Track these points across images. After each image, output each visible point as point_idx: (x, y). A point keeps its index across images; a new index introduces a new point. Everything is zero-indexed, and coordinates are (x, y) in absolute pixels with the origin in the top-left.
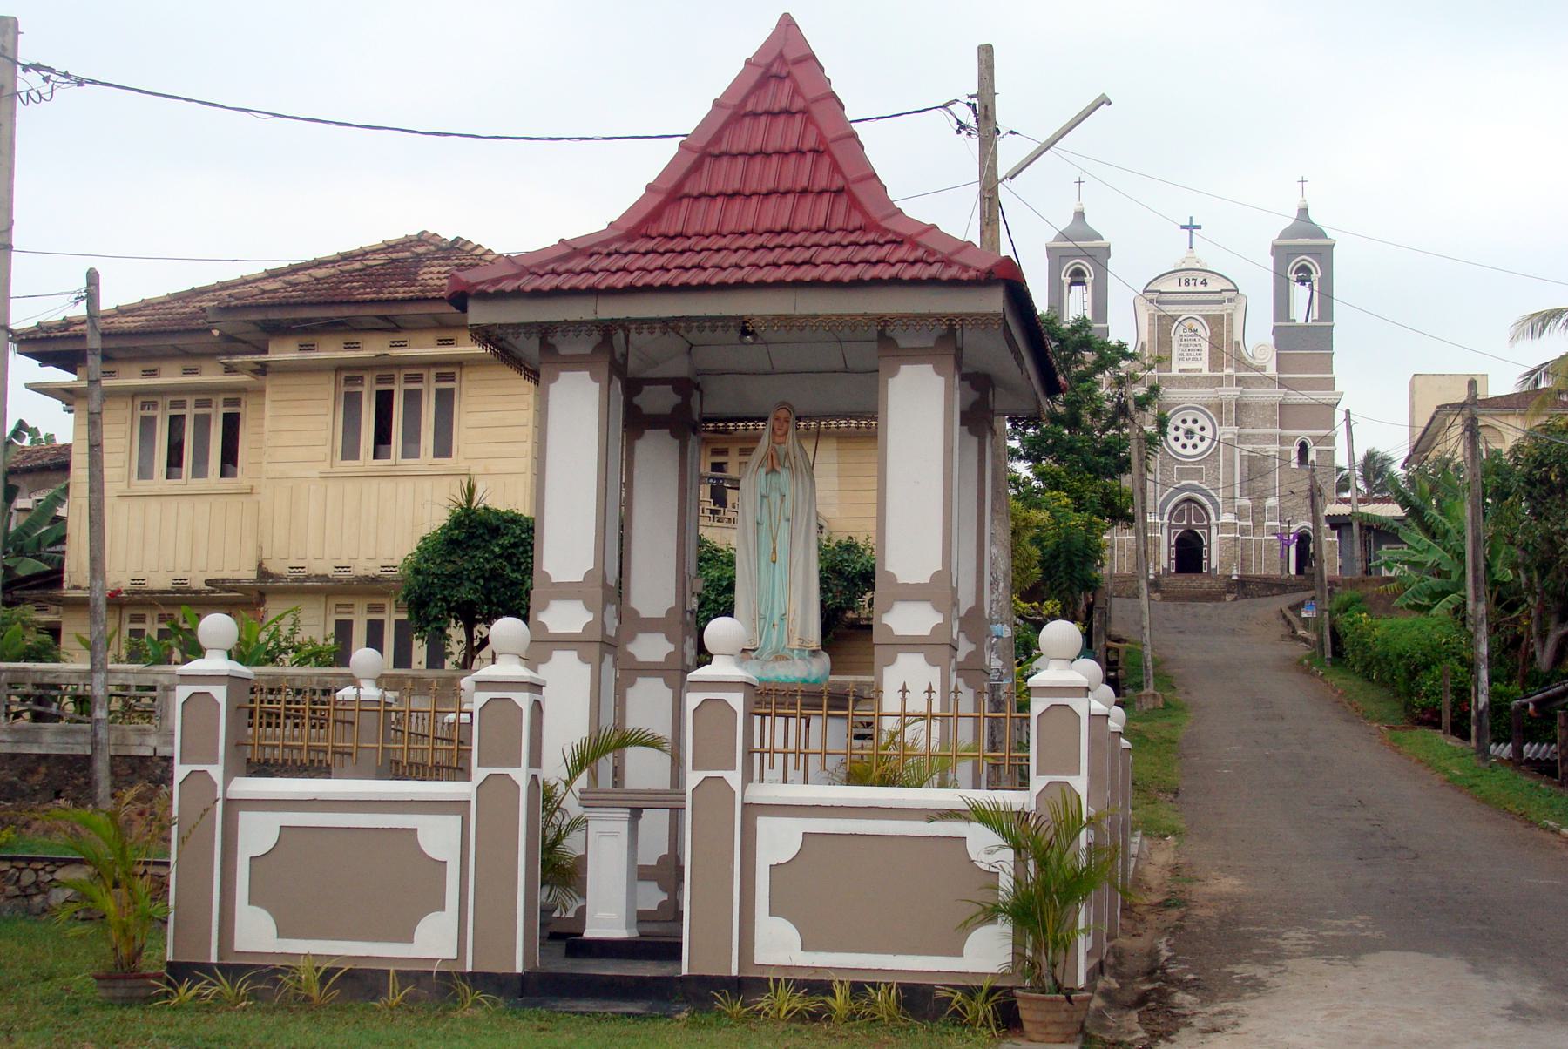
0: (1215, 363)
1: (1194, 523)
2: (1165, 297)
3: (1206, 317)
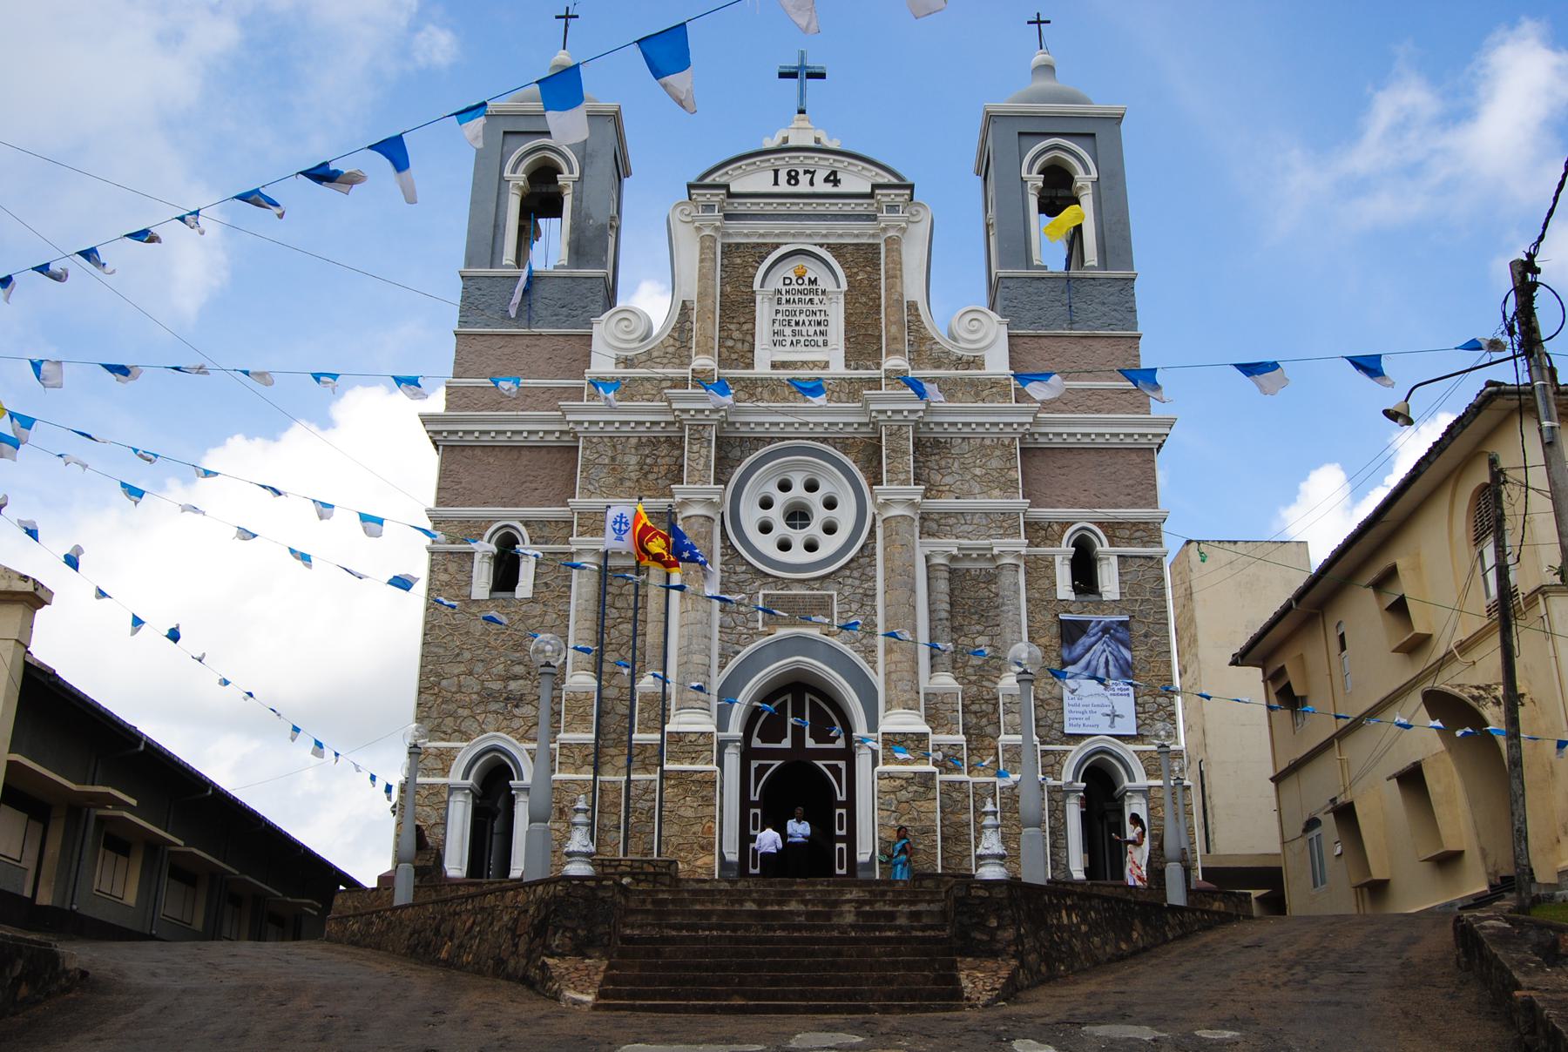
0: (863, 344)
1: (810, 743)
2: (739, 206)
3: (836, 249)
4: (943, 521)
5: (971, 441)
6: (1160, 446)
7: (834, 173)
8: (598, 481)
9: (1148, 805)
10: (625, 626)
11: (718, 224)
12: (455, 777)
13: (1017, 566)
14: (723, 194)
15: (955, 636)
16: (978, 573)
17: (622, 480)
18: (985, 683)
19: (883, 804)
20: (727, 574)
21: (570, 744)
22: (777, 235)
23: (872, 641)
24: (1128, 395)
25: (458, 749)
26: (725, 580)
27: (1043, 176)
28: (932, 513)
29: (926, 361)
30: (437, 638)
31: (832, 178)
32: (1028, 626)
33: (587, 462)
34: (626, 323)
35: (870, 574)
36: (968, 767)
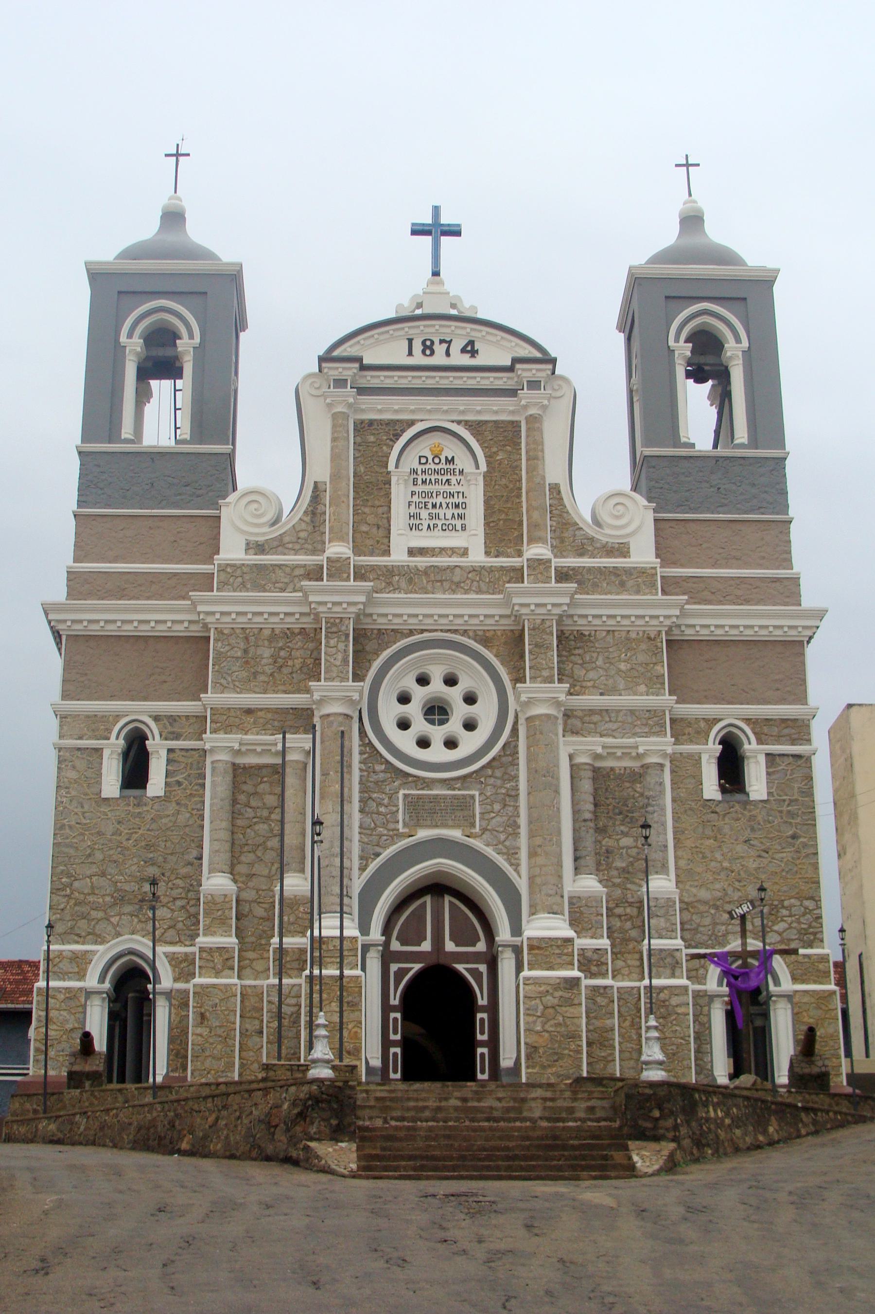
1: (450, 946)
3: (476, 427)
4: (587, 719)
5: (616, 634)
6: (811, 638)
7: (471, 343)
8: (230, 675)
9: (793, 1010)
10: (261, 826)
11: (351, 400)
12: (91, 981)
13: (662, 765)
14: (356, 368)
15: (599, 838)
16: (622, 772)
17: (255, 674)
18: (629, 886)
19: (528, 1009)
20: (365, 773)
21: (211, 949)
22: (413, 412)
23: (514, 843)
24: (778, 584)
25: (94, 953)
26: (364, 779)
27: (691, 345)
28: (576, 710)
29: (569, 548)
30: (67, 838)
31: (469, 348)
32: (674, 827)
33: (219, 655)
34: (255, 506)
35: (513, 773)
36: (613, 971)
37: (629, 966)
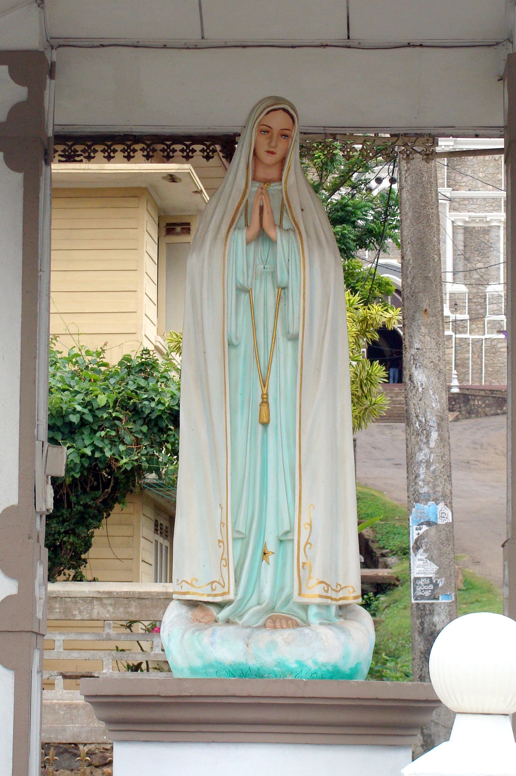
4: (461, 203)
36: (470, 330)
37: (478, 328)
